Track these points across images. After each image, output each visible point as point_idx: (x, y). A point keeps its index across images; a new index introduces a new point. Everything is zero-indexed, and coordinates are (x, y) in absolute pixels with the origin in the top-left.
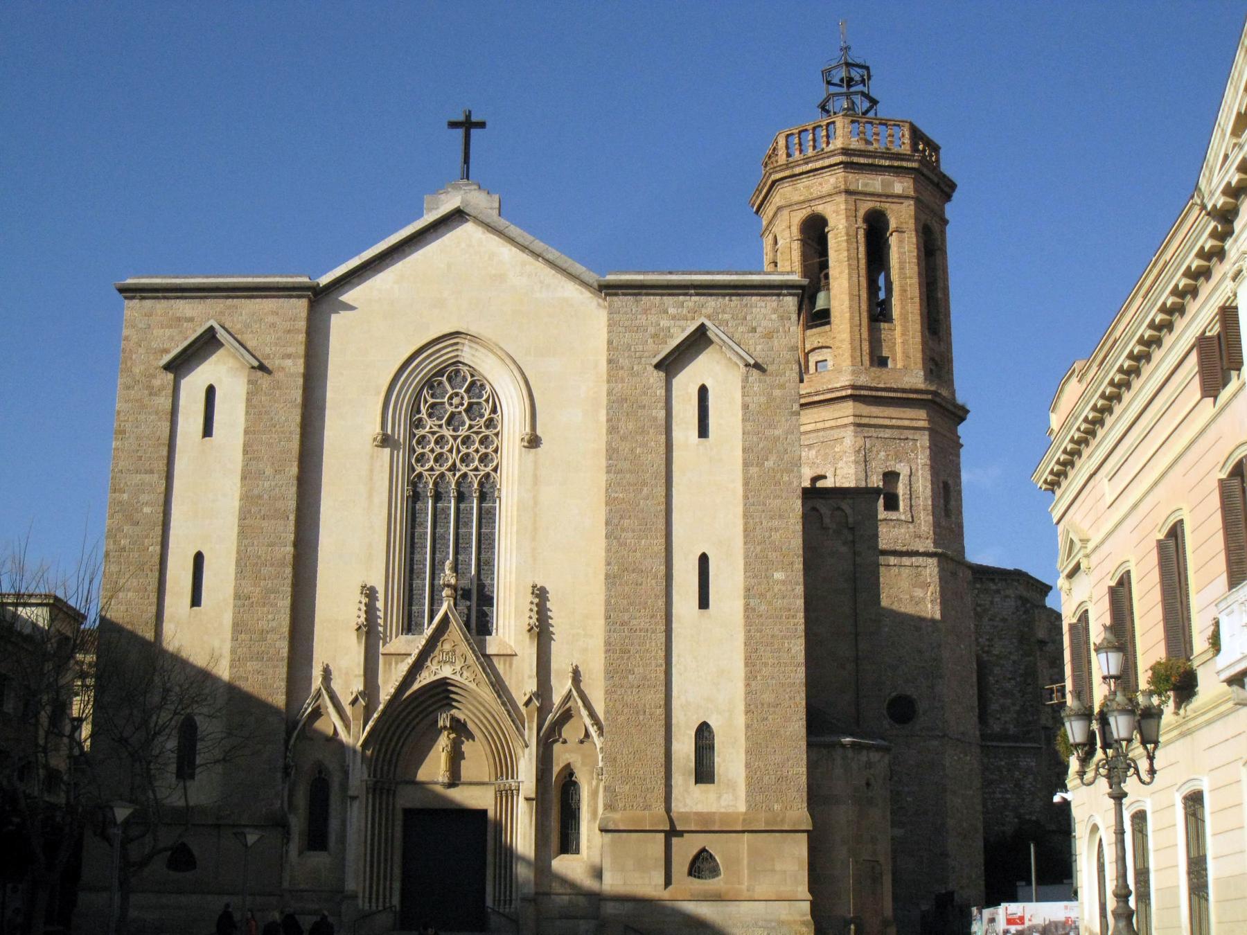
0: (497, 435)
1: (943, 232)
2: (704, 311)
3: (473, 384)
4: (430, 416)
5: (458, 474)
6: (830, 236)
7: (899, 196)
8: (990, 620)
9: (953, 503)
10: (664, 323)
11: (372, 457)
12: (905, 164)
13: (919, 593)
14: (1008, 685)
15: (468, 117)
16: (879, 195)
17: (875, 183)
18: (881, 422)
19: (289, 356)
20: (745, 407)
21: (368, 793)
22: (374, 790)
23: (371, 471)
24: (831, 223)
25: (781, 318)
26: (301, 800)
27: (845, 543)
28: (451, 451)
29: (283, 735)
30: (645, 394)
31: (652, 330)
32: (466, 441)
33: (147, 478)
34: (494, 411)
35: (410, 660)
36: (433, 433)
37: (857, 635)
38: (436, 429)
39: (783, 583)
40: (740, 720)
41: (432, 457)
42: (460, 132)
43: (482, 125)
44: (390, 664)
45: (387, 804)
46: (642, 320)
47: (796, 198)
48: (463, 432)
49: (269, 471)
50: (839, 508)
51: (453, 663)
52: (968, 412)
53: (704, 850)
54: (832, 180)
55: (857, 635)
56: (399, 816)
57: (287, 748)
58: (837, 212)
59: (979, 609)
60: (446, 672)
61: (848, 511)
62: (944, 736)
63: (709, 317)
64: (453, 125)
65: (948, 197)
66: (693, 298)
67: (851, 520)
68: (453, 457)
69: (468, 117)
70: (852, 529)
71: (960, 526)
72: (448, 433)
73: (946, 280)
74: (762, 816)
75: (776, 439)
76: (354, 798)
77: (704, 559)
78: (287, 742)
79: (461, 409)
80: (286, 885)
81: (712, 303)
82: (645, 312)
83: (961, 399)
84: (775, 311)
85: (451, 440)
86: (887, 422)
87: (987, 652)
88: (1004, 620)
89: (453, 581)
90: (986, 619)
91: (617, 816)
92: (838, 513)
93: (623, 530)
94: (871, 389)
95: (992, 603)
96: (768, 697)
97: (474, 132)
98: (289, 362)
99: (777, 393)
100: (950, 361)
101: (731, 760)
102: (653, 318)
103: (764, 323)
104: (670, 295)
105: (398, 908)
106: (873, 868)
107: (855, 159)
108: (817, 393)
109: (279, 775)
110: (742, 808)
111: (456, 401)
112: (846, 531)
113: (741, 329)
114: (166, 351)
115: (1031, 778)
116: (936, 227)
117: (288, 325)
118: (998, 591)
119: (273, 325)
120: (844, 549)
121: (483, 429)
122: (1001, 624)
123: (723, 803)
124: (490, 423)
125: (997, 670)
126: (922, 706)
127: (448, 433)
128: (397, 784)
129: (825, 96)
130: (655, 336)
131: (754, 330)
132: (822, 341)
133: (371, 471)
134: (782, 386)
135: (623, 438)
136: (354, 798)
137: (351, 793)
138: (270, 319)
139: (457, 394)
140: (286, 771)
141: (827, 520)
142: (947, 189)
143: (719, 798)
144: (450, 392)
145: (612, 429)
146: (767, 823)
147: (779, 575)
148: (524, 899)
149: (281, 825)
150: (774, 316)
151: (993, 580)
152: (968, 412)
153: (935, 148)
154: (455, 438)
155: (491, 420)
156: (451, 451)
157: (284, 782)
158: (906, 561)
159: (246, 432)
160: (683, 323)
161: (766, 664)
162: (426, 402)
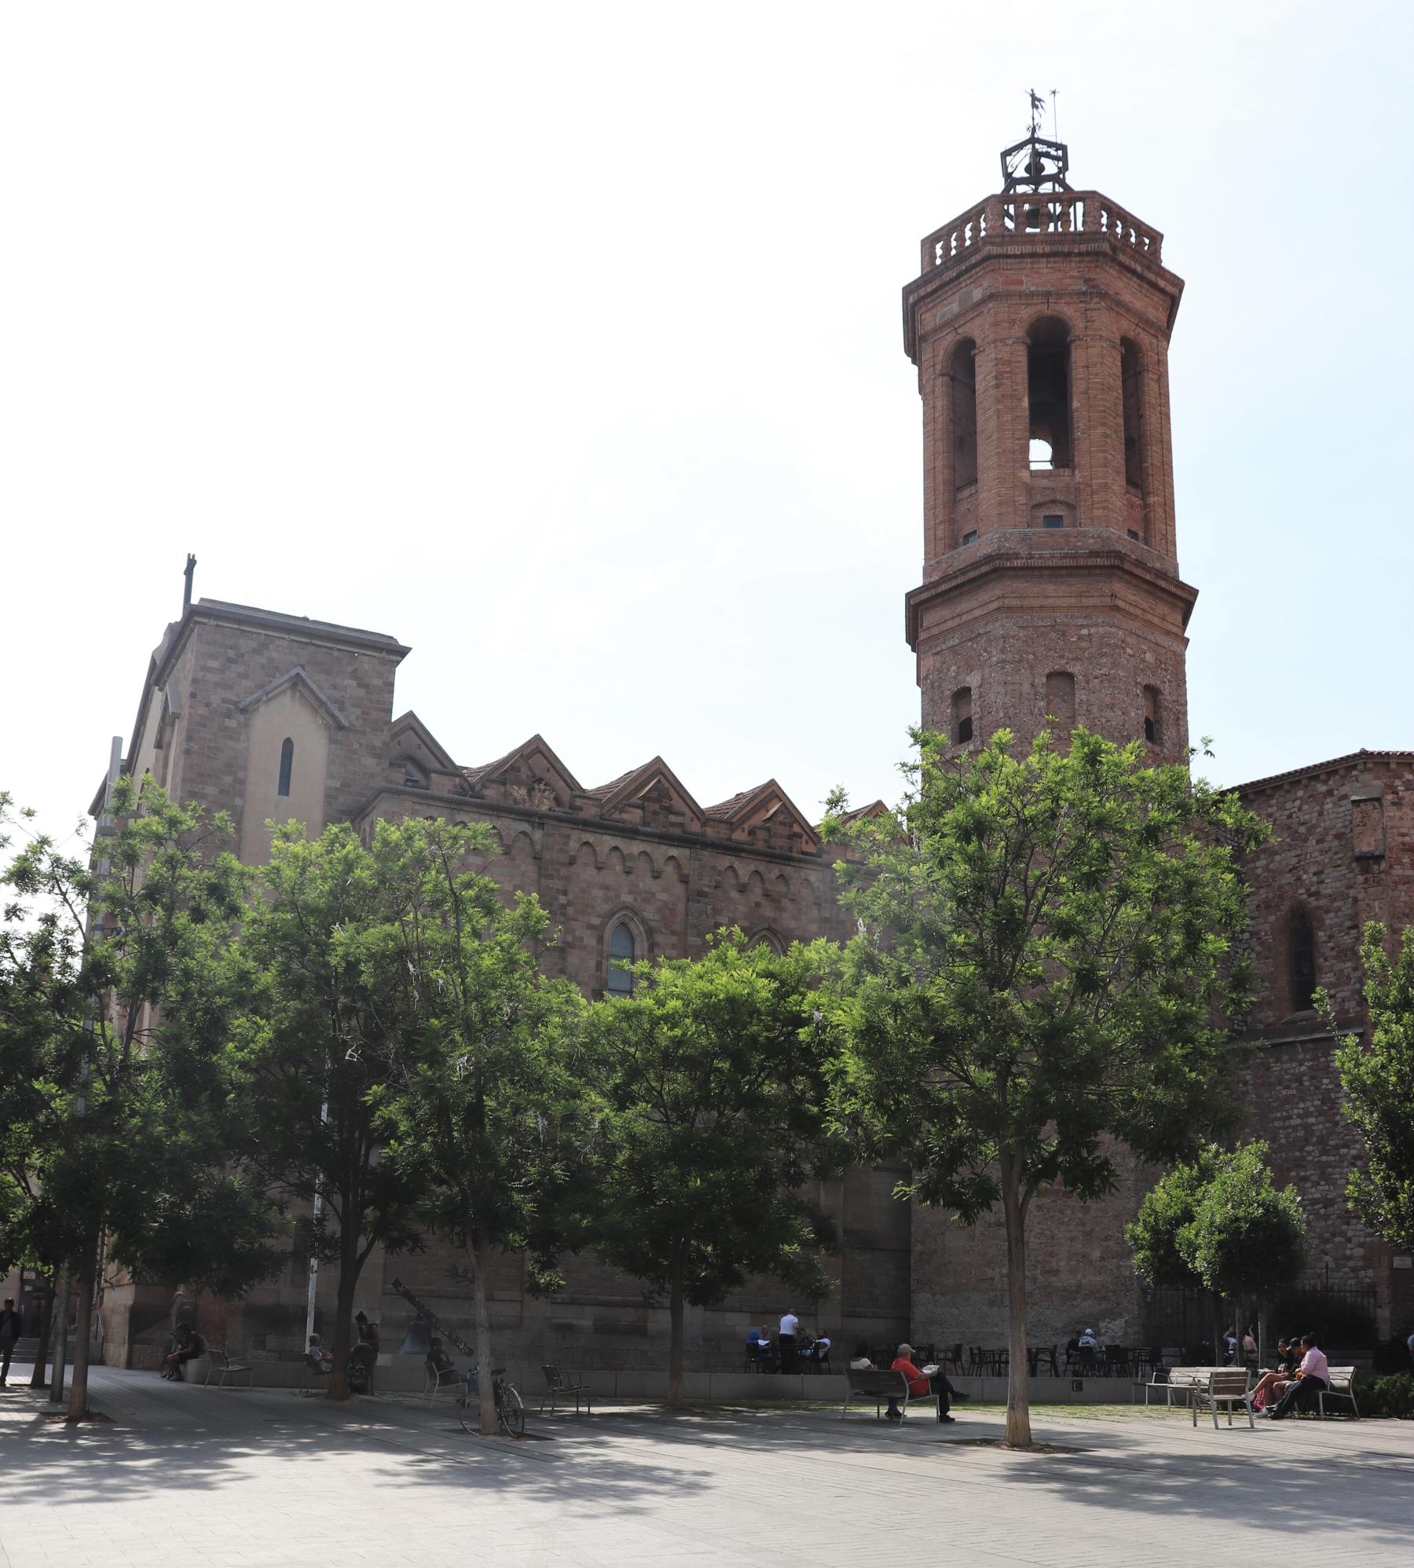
8: (1319, 842)
12: (973, 260)
18: (950, 624)
59: (1302, 829)
86: (957, 621)
87: (1317, 894)
90: (1312, 842)
95: (1321, 814)
118: (1330, 793)
122: (1336, 843)
125: (1329, 920)
151: (1316, 778)
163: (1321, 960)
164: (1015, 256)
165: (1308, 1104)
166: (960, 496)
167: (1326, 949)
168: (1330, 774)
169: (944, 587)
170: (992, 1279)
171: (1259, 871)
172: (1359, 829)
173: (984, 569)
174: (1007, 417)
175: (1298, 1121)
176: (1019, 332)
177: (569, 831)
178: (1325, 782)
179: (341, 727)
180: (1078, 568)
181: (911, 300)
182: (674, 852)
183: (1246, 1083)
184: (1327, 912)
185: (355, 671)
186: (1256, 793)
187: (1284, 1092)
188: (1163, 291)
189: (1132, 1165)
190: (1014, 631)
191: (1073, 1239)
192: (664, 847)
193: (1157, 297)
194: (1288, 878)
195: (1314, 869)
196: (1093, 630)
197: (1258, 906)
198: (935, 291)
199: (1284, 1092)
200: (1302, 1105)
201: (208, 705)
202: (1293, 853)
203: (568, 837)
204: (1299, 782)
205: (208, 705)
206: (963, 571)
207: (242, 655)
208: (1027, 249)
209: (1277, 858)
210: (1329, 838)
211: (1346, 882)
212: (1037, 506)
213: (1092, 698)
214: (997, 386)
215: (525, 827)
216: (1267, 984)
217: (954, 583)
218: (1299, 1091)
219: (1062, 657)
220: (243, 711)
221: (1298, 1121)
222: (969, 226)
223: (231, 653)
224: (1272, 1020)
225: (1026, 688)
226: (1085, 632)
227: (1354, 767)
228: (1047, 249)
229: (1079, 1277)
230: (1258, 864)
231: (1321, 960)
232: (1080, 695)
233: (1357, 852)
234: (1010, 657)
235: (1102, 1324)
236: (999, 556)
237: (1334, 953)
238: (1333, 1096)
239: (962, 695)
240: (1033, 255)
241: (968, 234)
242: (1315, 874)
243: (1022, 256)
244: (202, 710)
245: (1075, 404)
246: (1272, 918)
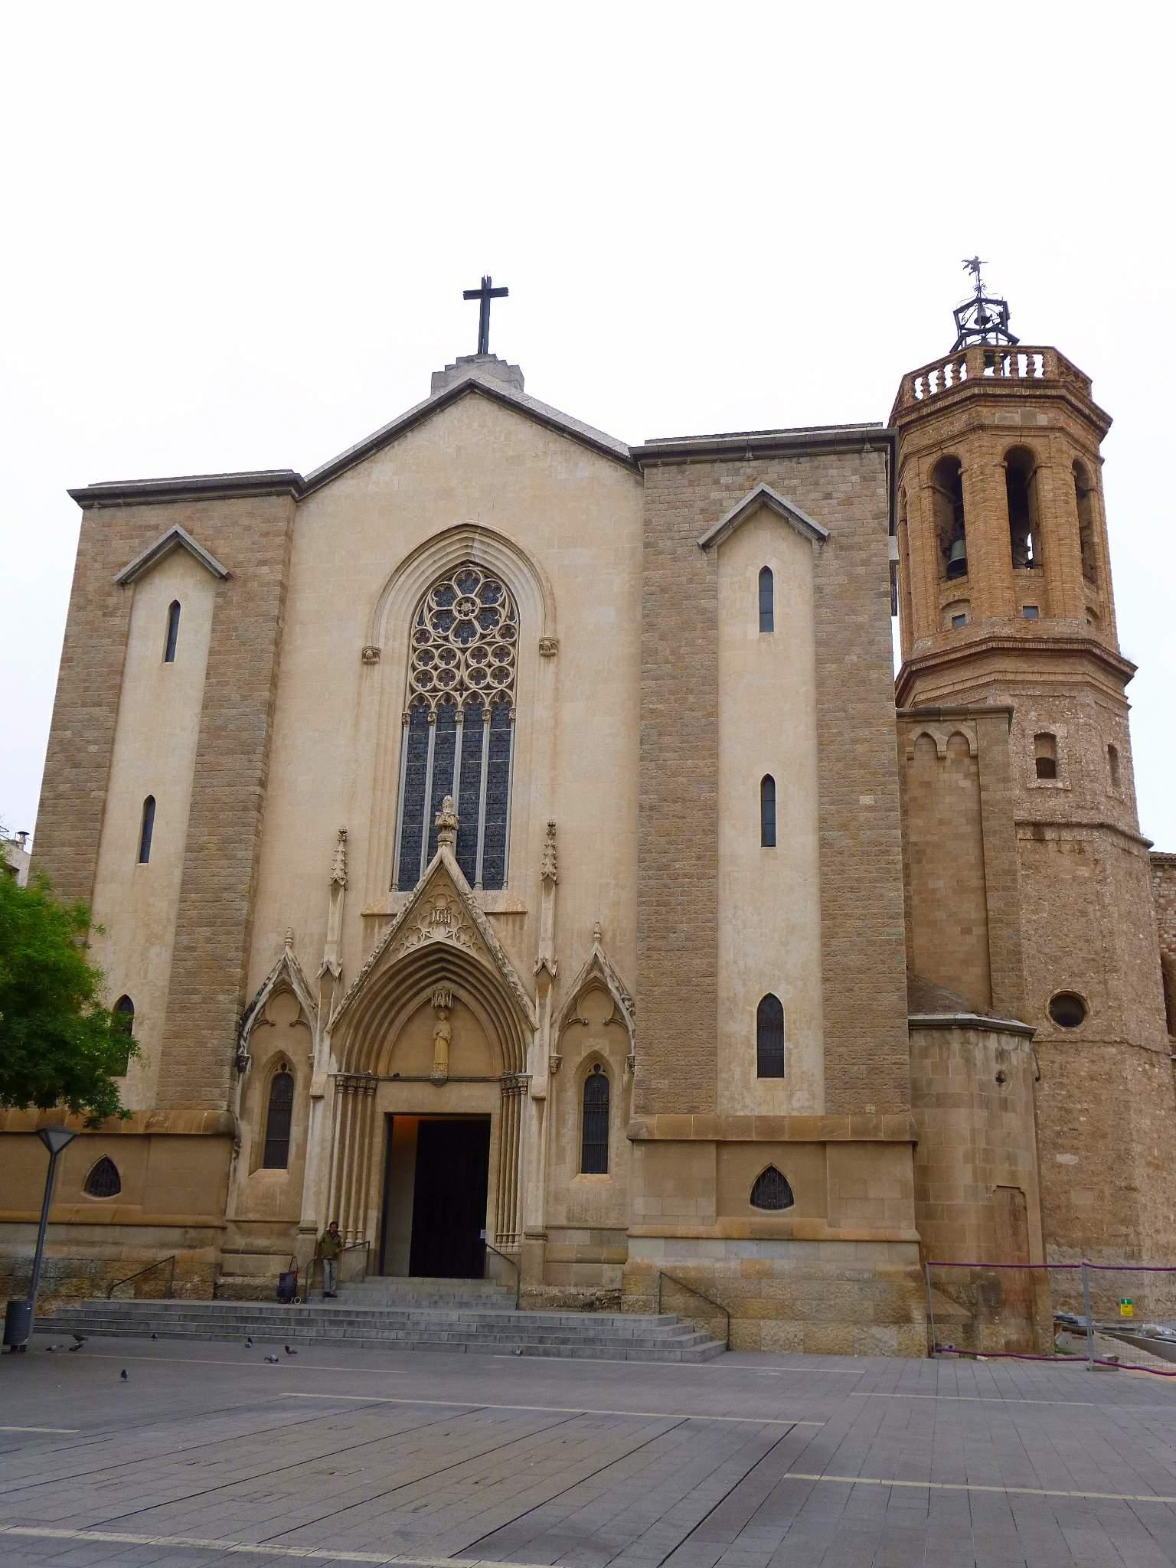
0: (513, 644)
1: (1098, 472)
2: (765, 477)
3: (486, 585)
4: (435, 626)
5: (465, 694)
6: (964, 478)
7: (1045, 429)
9: (1121, 770)
10: (715, 495)
11: (361, 677)
12: (1049, 392)
13: (1084, 872)
15: (486, 282)
16: (1021, 428)
17: (1014, 416)
18: (1030, 677)
19: (264, 563)
20: (818, 590)
21: (336, 1093)
22: (346, 1088)
23: (359, 694)
24: (965, 464)
25: (864, 479)
26: (258, 1099)
27: (966, 776)
28: (458, 667)
29: (235, 1017)
30: (690, 581)
31: (700, 504)
32: (479, 654)
33: (96, 711)
34: (511, 617)
35: (399, 919)
36: (437, 647)
37: (985, 890)
38: (441, 642)
39: (869, 808)
40: (815, 991)
41: (435, 674)
42: (478, 302)
43: (503, 292)
44: (373, 929)
45: (364, 1109)
46: (687, 493)
47: (926, 442)
48: (473, 643)
49: (236, 697)
50: (958, 734)
51: (446, 924)
52: (1134, 668)
53: (771, 1169)
54: (965, 417)
55: (985, 890)
56: (380, 1122)
57: (240, 1035)
58: (970, 451)
59: (1162, 901)
60: (439, 935)
61: (969, 735)
62: (1121, 1043)
63: (772, 484)
64: (469, 295)
65: (1103, 433)
66: (753, 463)
67: (973, 746)
68: (462, 674)
69: (486, 282)
70: (975, 758)
71: (1133, 800)
72: (455, 644)
73: (1103, 523)
74: (849, 1120)
75: (860, 627)
76: (318, 1098)
77: (768, 782)
78: (240, 1027)
79: (471, 616)
80: (231, 1214)
81: (775, 469)
82: (691, 484)
83: (1126, 652)
84: (855, 472)
85: (458, 653)
86: (1037, 677)
89: (452, 821)
91: (652, 1121)
92: (958, 739)
93: (661, 750)
94: (1015, 640)
96: (855, 959)
97: (495, 302)
98: (265, 569)
99: (861, 570)
100: (1112, 613)
101: (803, 1046)
102: (700, 491)
103: (844, 487)
104: (722, 461)
105: (372, 1246)
106: (1013, 1197)
107: (990, 390)
108: (954, 650)
109: (227, 1069)
110: (819, 1109)
111: (467, 606)
112: (967, 761)
113: (813, 495)
114: (125, 564)
116: (1090, 466)
117: (265, 527)
119: (247, 528)
120: (967, 784)
121: (498, 639)
123: (796, 1104)
124: (508, 632)
126: (1092, 1006)
127: (455, 644)
128: (377, 1080)
129: (956, 339)
130: (702, 511)
131: (828, 496)
132: (958, 594)
133: (359, 694)
134: (864, 563)
135: (662, 638)
136: (318, 1098)
137: (315, 1090)
138: (246, 521)
139: (467, 600)
140: (239, 1064)
141: (942, 748)
142: (1101, 424)
143: (791, 1096)
144: (460, 595)
145: (651, 627)
146: (855, 1131)
147: (867, 800)
148: (530, 1236)
149: (229, 1136)
150: (855, 478)
152: (1134, 668)
153: (1086, 382)
154: (464, 651)
155: (508, 628)
156: (458, 667)
157: (233, 1078)
158: (1066, 835)
159: (212, 652)
160: (737, 493)
161: (849, 916)
162: (430, 609)
169: (1032, 645)
173: (1076, 646)
206: (1056, 641)
217: (1043, 646)
239: (1046, 738)
240: (1079, 411)
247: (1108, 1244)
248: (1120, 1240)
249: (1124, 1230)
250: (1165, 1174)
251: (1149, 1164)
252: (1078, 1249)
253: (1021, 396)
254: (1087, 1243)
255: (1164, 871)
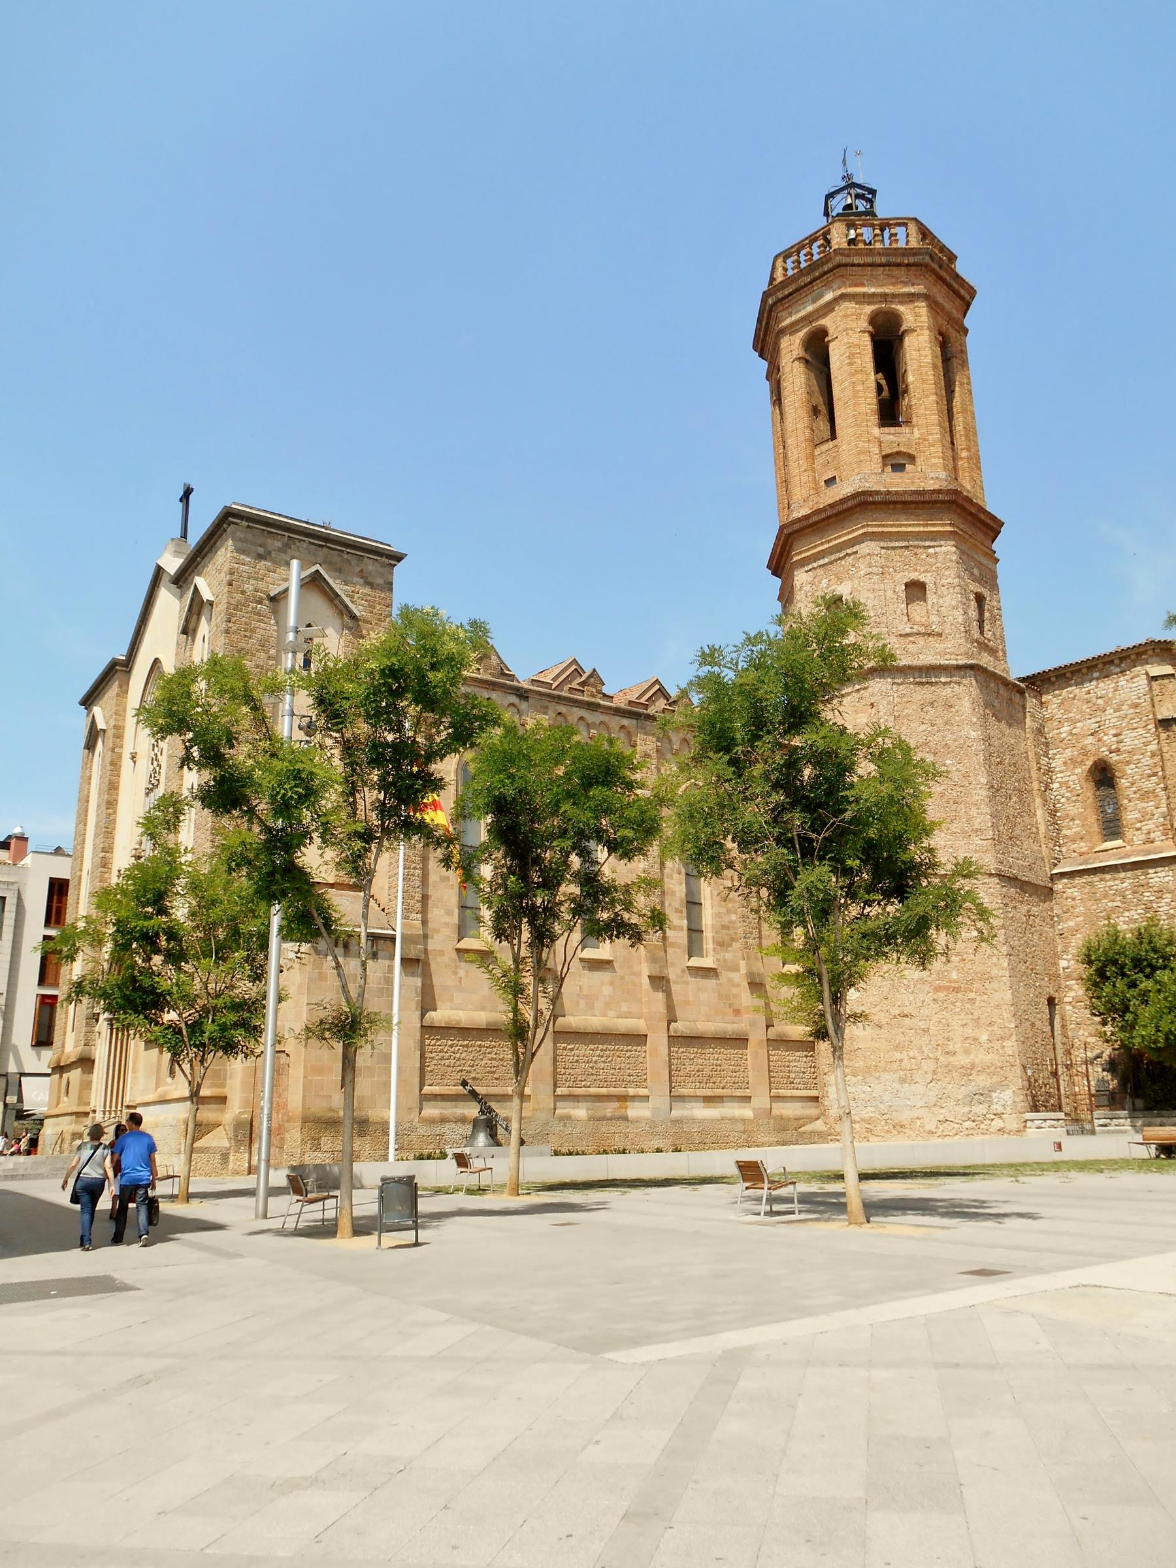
12: (826, 268)
14: (1149, 785)
59: (1100, 701)
87: (1118, 750)
88: (1136, 706)
115: (1168, 897)
122: (1132, 711)
151: (1111, 662)
163: (1126, 801)
164: (859, 265)
165: (1132, 912)
166: (817, 452)
167: (1129, 792)
168: (1122, 659)
169: (815, 519)
170: (901, 1060)
171: (1064, 735)
172: (1159, 698)
173: (850, 503)
174: (860, 388)
175: (1125, 927)
176: (864, 324)
177: (547, 704)
178: (1119, 666)
179: (353, 617)
180: (923, 502)
181: (770, 301)
182: (625, 722)
183: (1074, 899)
184: (1128, 763)
185: (362, 571)
186: (1073, 673)
187: (1110, 904)
188: (962, 298)
189: (1006, 964)
190: (877, 550)
191: (964, 1025)
192: (617, 718)
193: (958, 302)
194: (1090, 740)
195: (1114, 732)
196: (937, 549)
197: (1065, 763)
198: (790, 294)
199: (1110, 904)
200: (1127, 914)
201: (243, 592)
202: (1093, 720)
203: (547, 707)
204: (1096, 666)
205: (243, 592)
207: (270, 553)
208: (869, 260)
209: (1079, 724)
210: (1125, 707)
211: (1144, 740)
212: (885, 457)
213: (941, 601)
214: (851, 364)
215: (513, 699)
216: (1077, 822)
217: (824, 515)
218: (1123, 903)
219: (916, 570)
220: (273, 599)
221: (1125, 927)
222: (803, 252)
223: (261, 550)
224: (1085, 849)
225: (890, 594)
226: (931, 550)
227: (1145, 652)
228: (884, 260)
229: (972, 1056)
230: (1062, 730)
231: (1126, 801)
232: (931, 597)
233: (1160, 717)
234: (875, 570)
235: (994, 1095)
236: (864, 493)
237: (1138, 795)
238: (1154, 905)
240: (873, 265)
241: (802, 258)
242: (1116, 735)
243: (864, 265)
244: (238, 596)
245: (910, 378)
246: (1078, 771)
247: (884, 1070)
248: (895, 1066)
249: (898, 1056)
250: (972, 995)
251: (937, 989)
252: (860, 1078)
253: (806, 285)
254: (868, 1070)
255: (1101, 671)
